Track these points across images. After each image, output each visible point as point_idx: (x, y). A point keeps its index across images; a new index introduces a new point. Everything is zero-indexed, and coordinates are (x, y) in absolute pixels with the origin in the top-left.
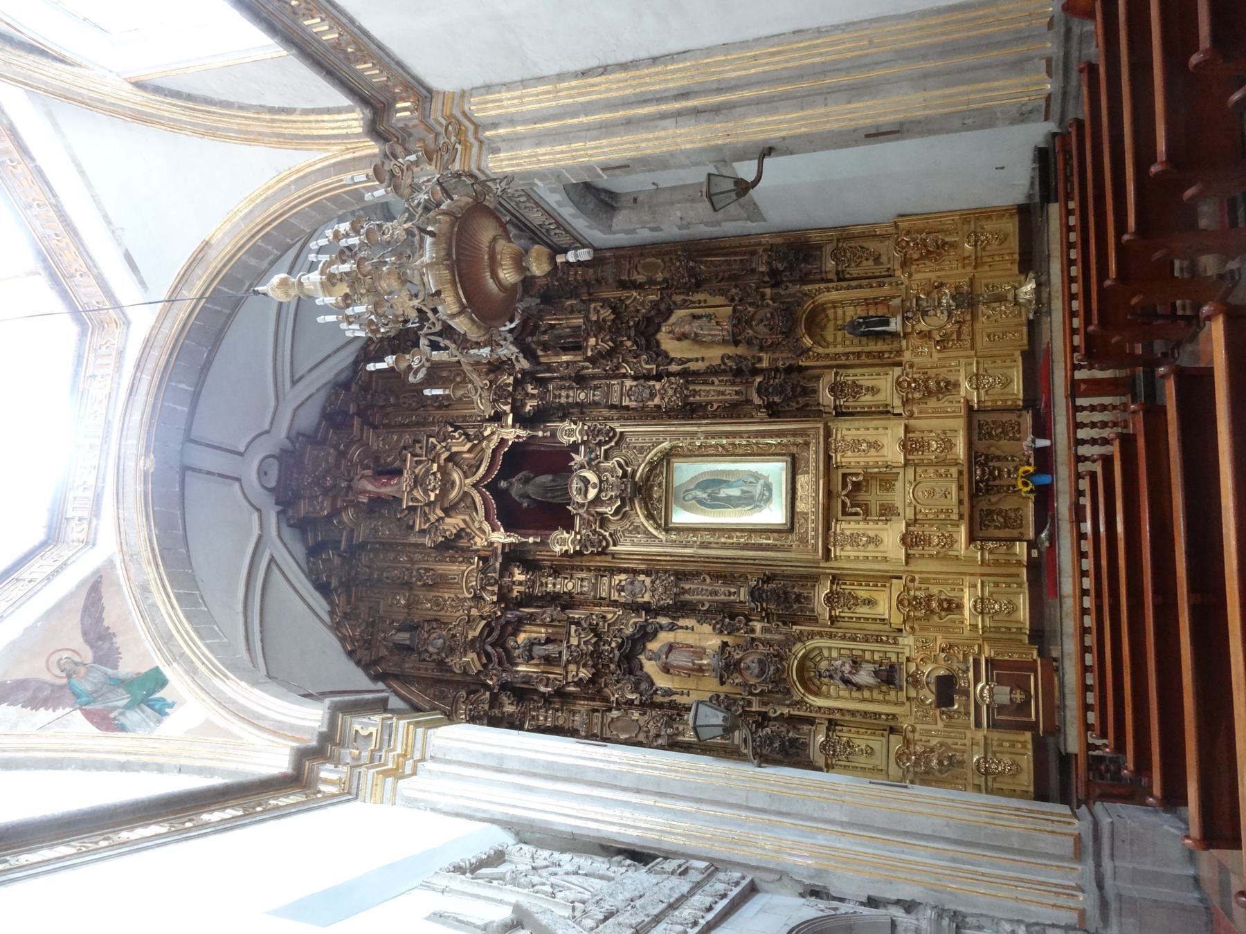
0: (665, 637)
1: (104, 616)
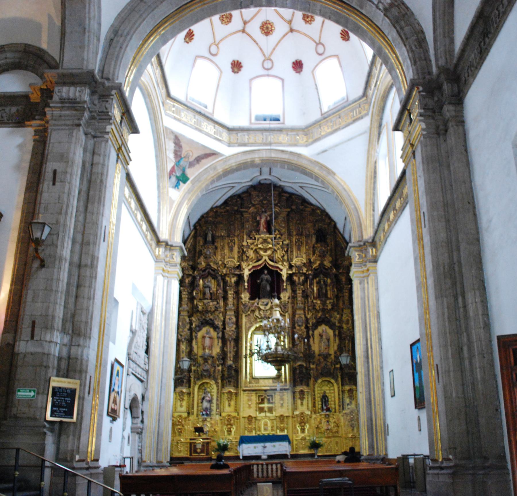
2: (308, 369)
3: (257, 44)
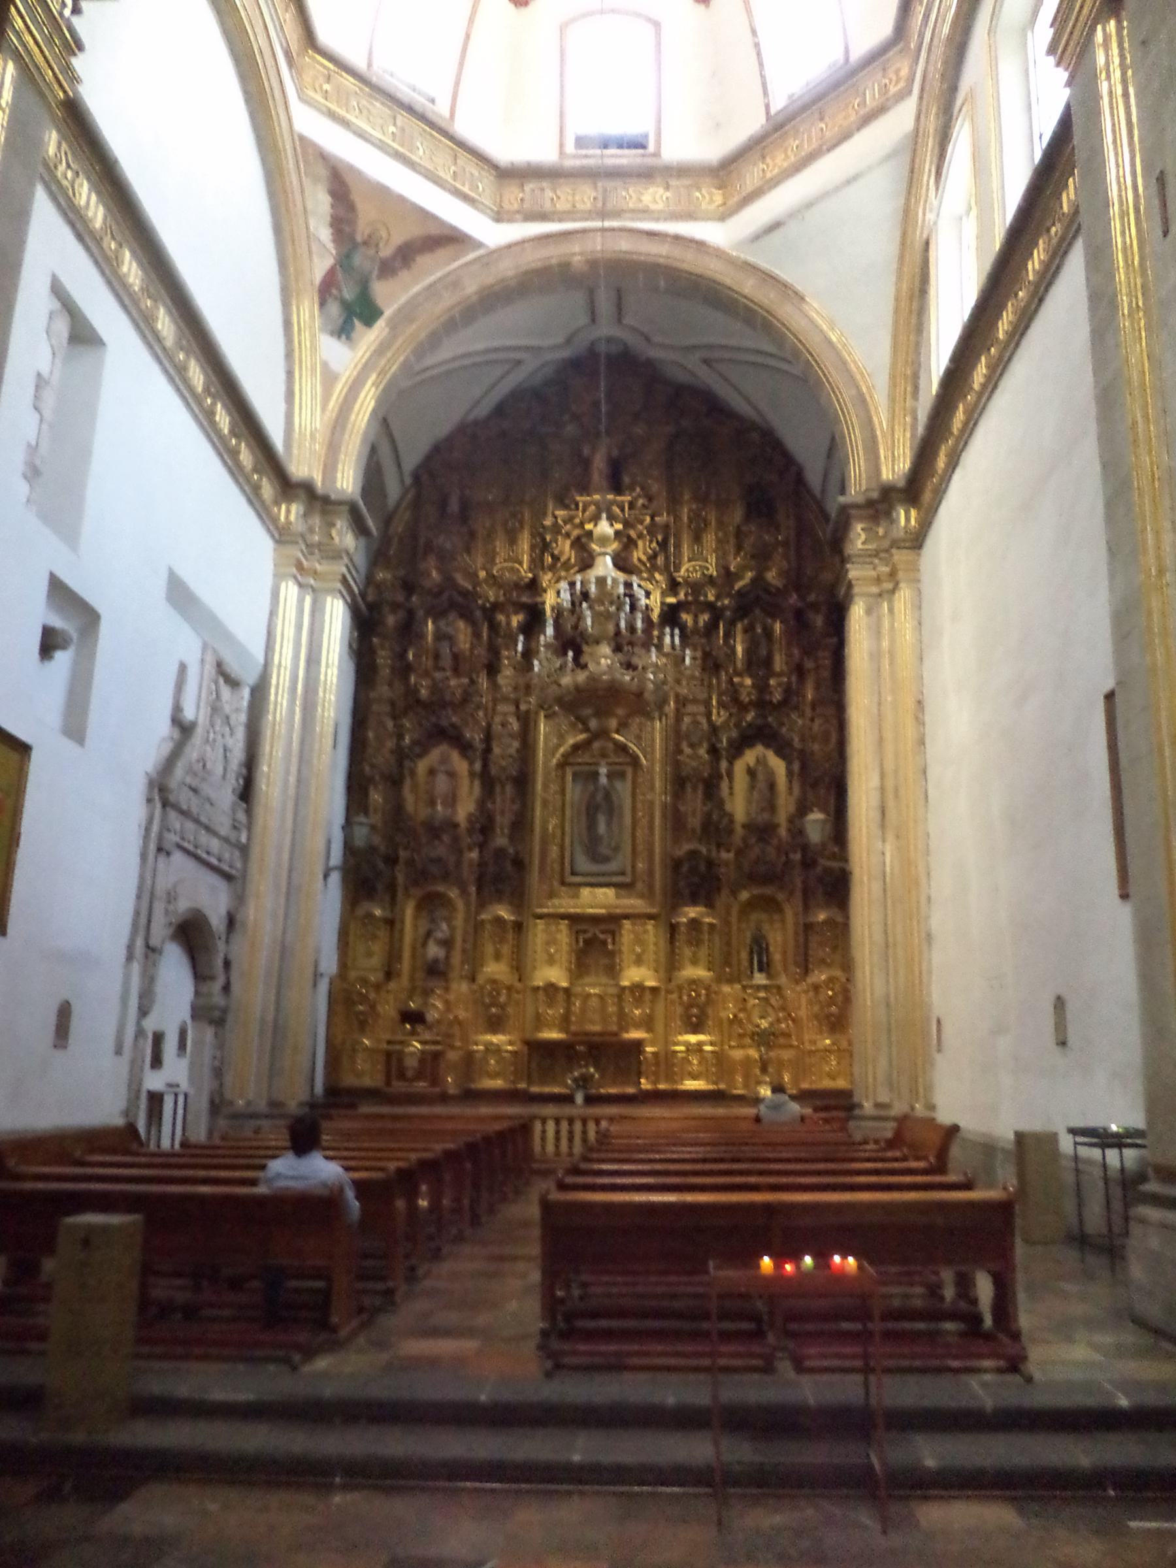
0: (460, 765)
2: (710, 863)
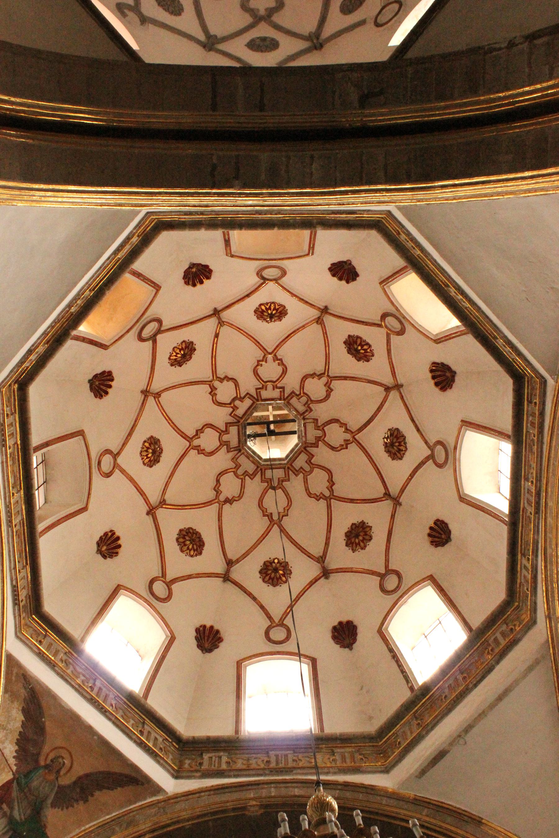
1: (105, 791)
3: (254, 599)
